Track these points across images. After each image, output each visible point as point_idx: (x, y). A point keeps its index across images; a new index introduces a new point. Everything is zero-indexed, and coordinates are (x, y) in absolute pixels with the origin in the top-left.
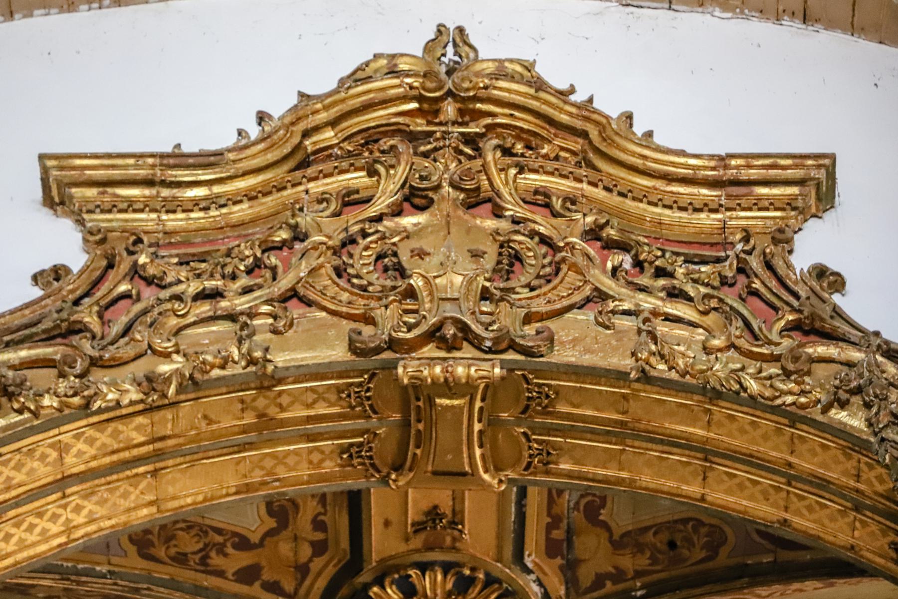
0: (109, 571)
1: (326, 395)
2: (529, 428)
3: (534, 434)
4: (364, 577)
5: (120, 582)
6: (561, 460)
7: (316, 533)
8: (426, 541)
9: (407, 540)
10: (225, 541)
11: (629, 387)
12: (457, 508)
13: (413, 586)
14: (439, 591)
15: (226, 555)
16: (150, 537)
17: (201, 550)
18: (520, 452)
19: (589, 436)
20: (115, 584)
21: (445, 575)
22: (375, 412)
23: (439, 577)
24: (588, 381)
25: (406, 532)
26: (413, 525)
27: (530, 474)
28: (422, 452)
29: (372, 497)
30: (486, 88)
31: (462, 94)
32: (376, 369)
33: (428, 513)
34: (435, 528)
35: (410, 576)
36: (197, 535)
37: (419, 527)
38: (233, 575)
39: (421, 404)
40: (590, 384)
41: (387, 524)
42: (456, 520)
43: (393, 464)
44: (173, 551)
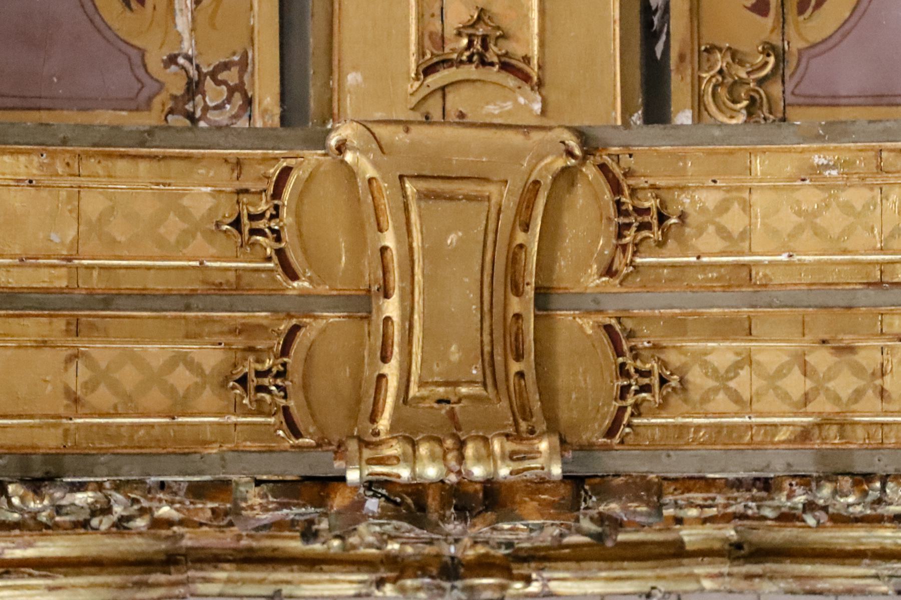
1: (711, 383)
2: (280, 291)
3: (271, 270)
6: (209, 202)
11: (66, 432)
18: (298, 216)
19: (155, 284)
22: (608, 328)
24: (156, 431)
27: (276, 159)
28: (512, 236)
30: (380, 583)
31: (427, 580)
32: (607, 448)
39: (515, 367)
40: (152, 426)
43: (573, 184)
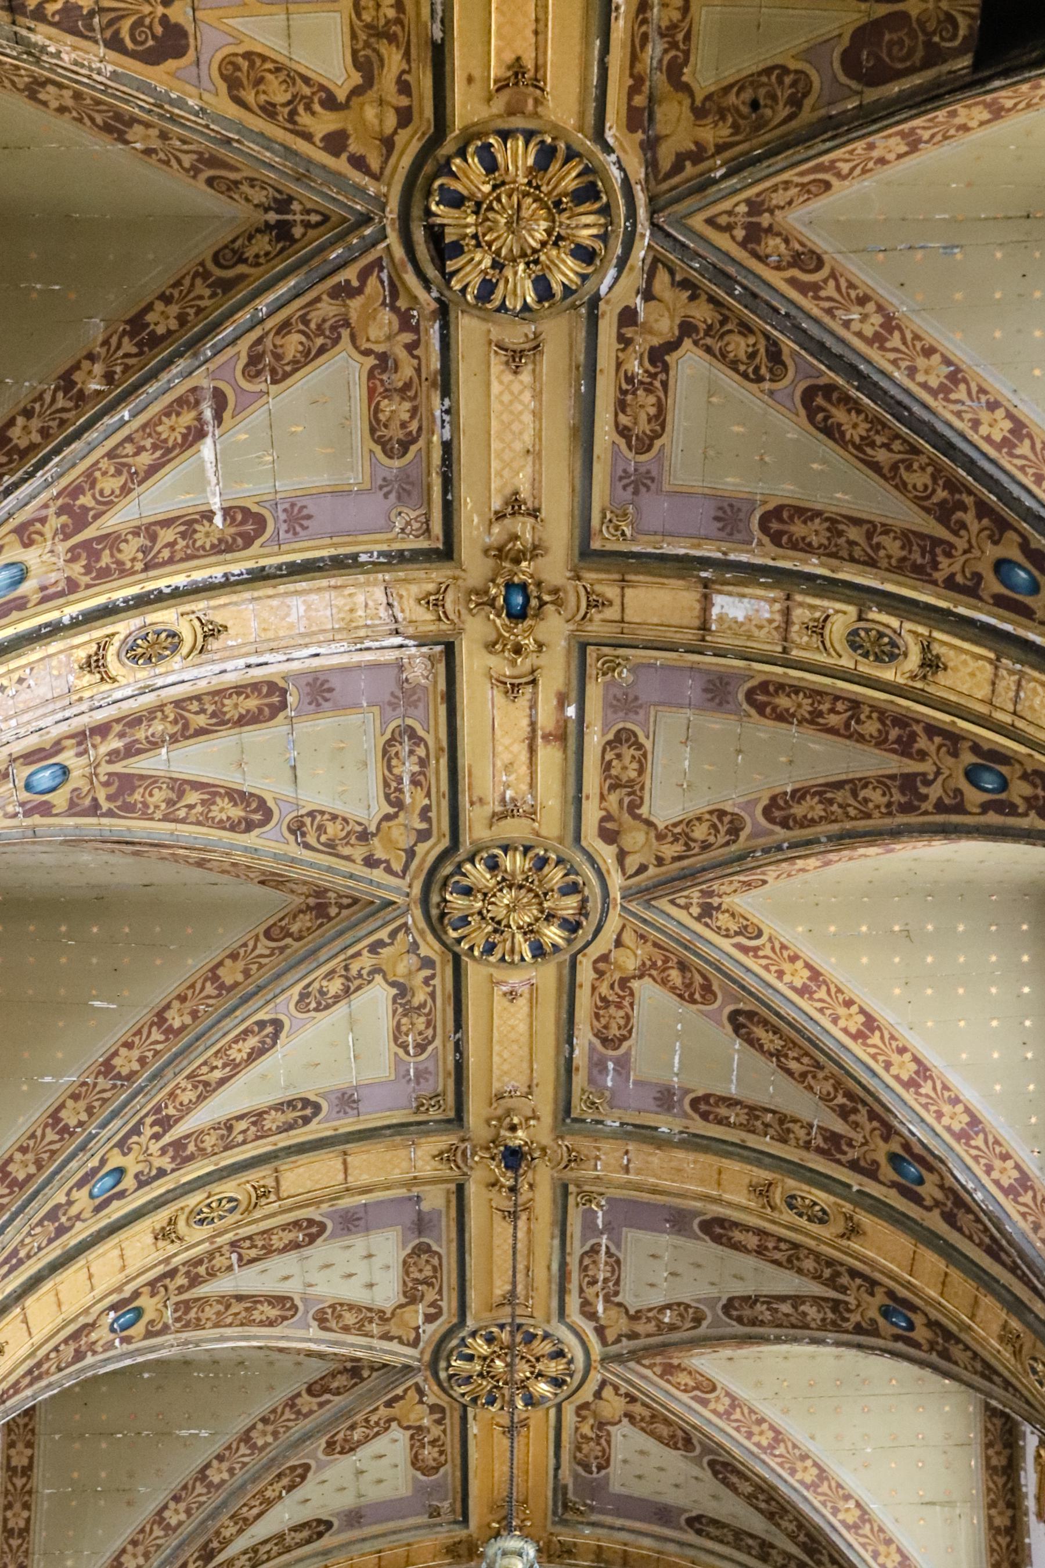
0: (201, 109)
4: (448, 147)
5: (212, 126)
7: (403, 97)
8: (508, 104)
9: (489, 100)
10: (313, 94)
12: (540, 62)
13: (494, 159)
14: (520, 163)
15: (313, 113)
16: (239, 74)
17: (289, 103)
20: (207, 127)
21: (527, 144)
23: (521, 143)
25: (490, 92)
26: (496, 82)
29: (456, 44)
33: (509, 68)
34: (516, 84)
35: (491, 145)
36: (285, 81)
37: (502, 86)
38: (323, 139)
41: (470, 80)
42: (537, 83)
44: (263, 98)
